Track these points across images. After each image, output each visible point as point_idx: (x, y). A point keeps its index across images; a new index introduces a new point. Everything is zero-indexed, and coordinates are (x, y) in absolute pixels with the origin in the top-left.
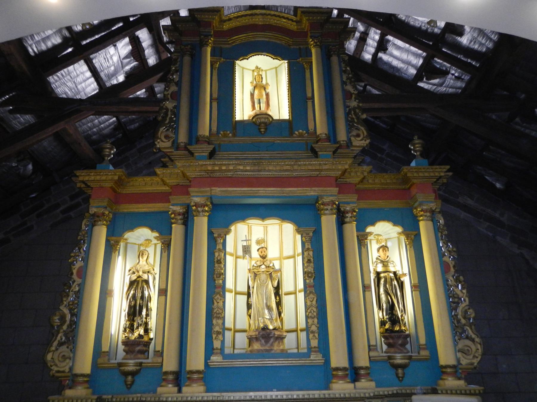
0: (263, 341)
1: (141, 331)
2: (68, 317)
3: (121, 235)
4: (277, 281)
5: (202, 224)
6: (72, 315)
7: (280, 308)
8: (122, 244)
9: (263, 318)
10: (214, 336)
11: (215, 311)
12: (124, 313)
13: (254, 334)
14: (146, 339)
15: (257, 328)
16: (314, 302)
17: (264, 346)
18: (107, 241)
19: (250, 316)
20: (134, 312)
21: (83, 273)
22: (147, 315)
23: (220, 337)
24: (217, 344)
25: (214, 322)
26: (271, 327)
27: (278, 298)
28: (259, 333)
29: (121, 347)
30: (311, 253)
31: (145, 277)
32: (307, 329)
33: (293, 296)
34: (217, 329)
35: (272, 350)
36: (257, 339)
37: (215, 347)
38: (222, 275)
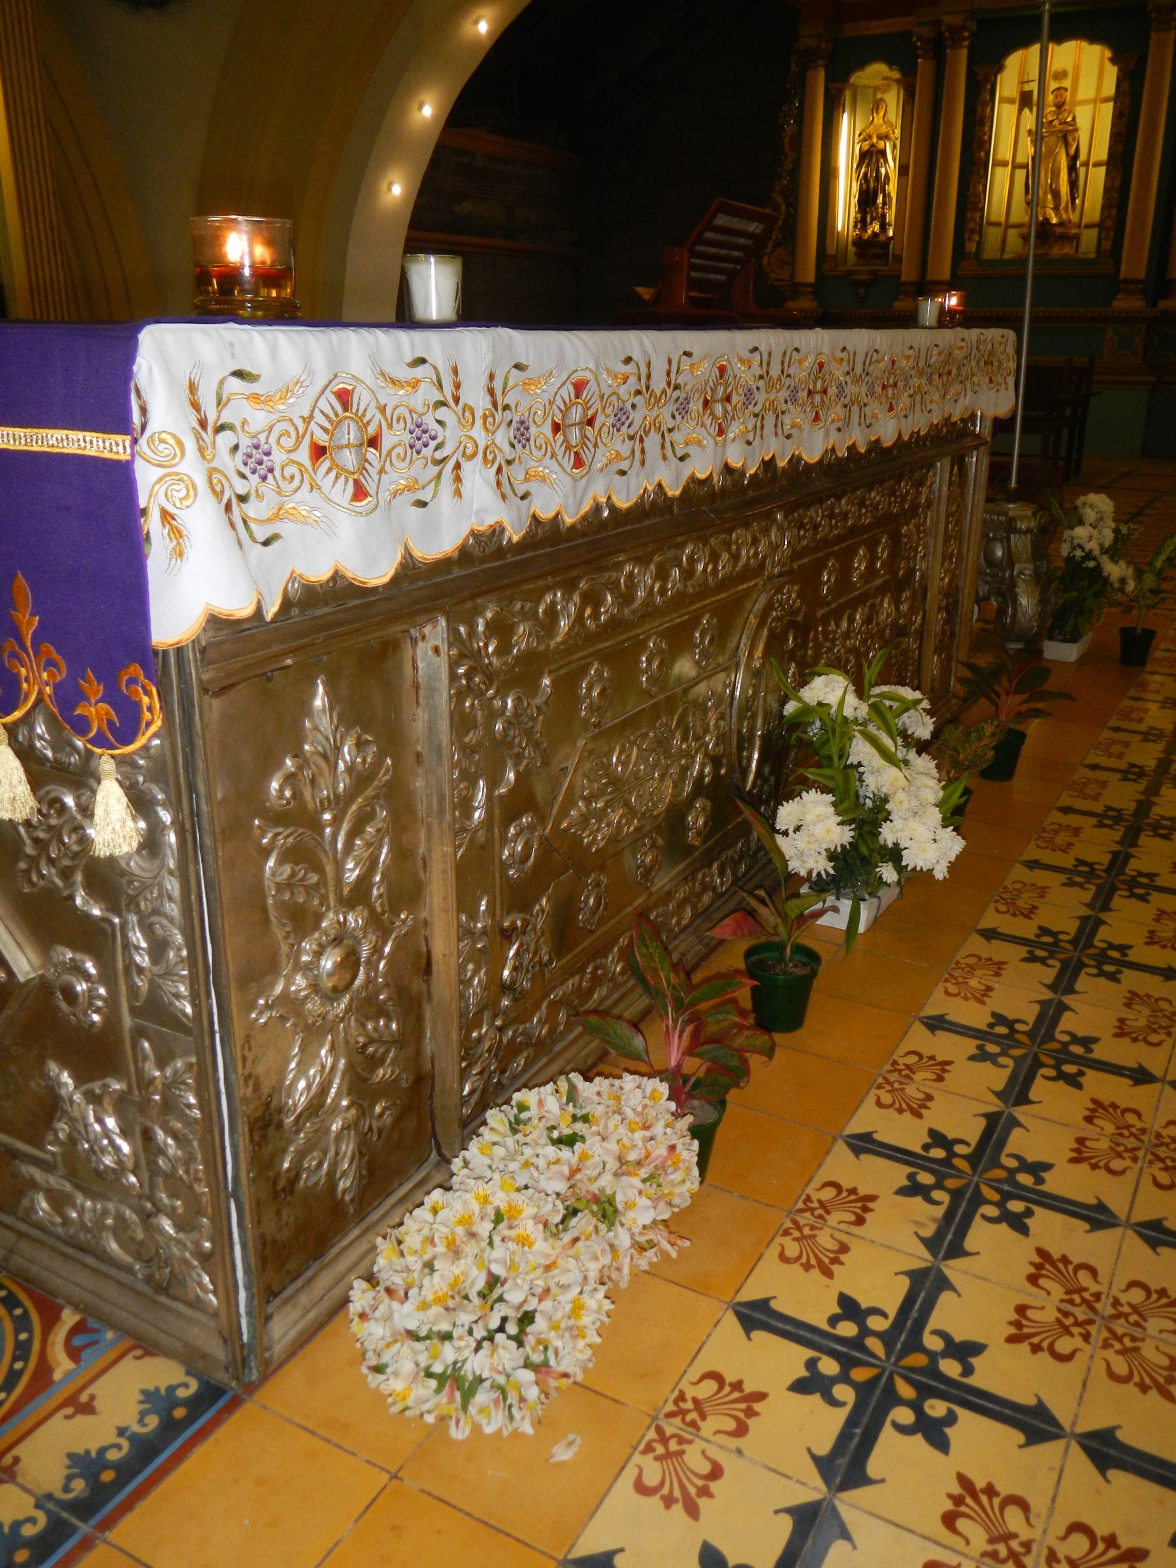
1: (876, 227)
2: (783, 206)
3: (845, 79)
5: (960, 60)
6: (789, 205)
8: (848, 94)
12: (855, 201)
14: (882, 238)
18: (827, 90)
20: (867, 199)
21: (799, 142)
22: (884, 203)
24: (971, 247)
26: (1054, 221)
29: (851, 249)
31: (881, 144)
32: (1100, 225)
34: (972, 225)
38: (984, 145)
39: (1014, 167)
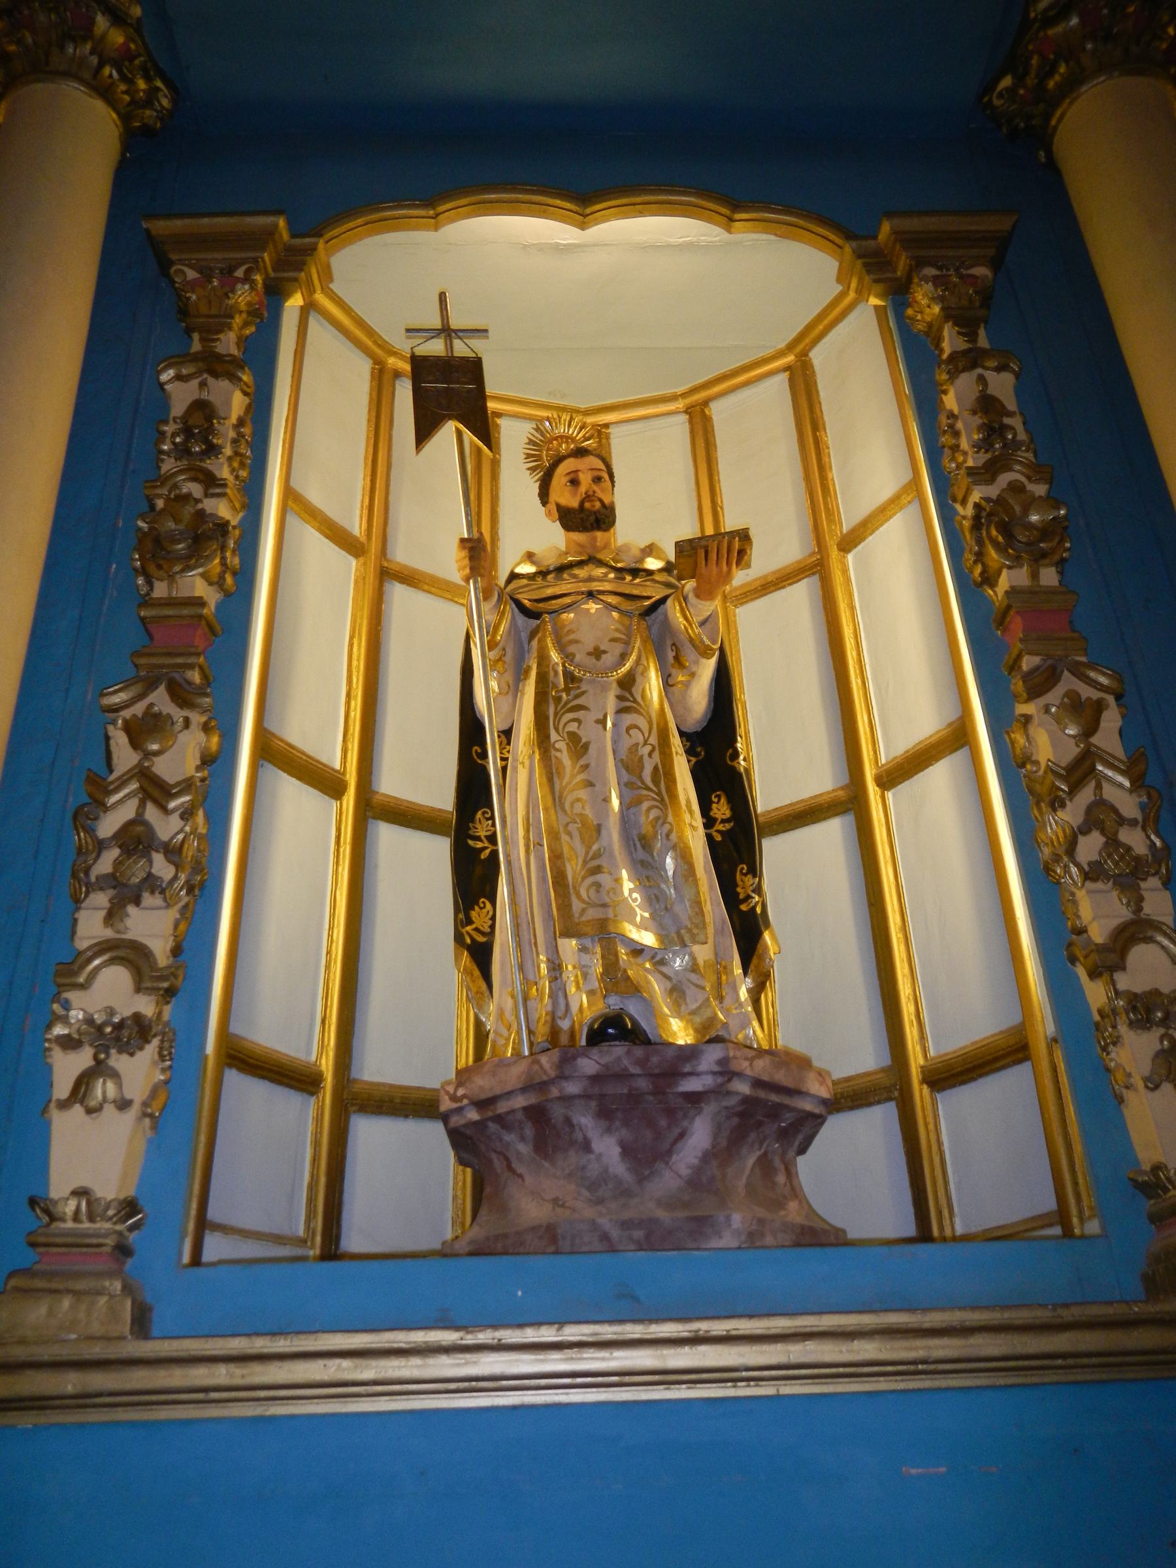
0: (607, 1149)
4: (708, 668)
7: (745, 883)
9: (604, 933)
10: (67, 1067)
11: (108, 826)
13: (515, 1076)
15: (542, 1030)
16: (1108, 737)
17: (624, 1193)
19: (480, 954)
23: (138, 1071)
25: (91, 926)
27: (721, 810)
28: (568, 1058)
30: (1002, 385)
33: (832, 833)
34: (111, 992)
35: (701, 1226)
36: (545, 1128)
37: (59, 1187)
39: (373, 809)
